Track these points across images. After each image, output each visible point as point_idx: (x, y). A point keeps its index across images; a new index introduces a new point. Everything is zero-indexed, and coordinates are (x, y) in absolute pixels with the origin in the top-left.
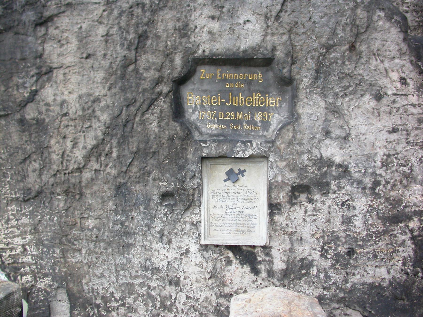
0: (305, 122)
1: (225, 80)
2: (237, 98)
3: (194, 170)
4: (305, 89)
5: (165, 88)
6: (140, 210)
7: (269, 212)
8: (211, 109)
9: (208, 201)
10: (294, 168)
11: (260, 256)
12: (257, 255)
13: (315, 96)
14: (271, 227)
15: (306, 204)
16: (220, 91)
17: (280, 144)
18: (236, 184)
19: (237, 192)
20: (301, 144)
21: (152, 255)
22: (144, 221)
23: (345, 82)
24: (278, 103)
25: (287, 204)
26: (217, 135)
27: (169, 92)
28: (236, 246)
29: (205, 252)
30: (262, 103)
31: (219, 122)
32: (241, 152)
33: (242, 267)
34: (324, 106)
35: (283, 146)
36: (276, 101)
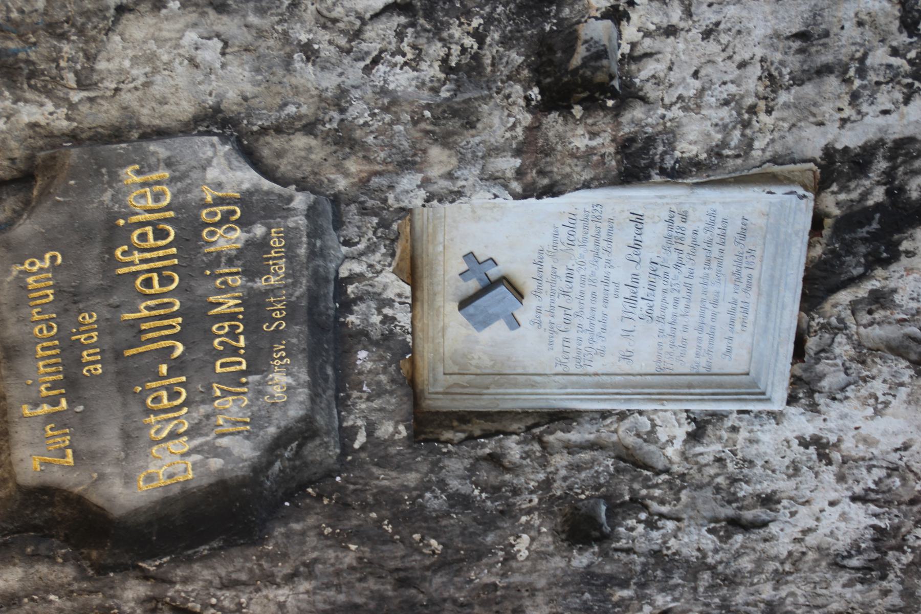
0: (234, 84)
1: (71, 383)
2: (144, 327)
3: (467, 463)
4: (72, 106)
6: (631, 599)
7: (657, 178)
8: (203, 402)
9: (601, 384)
10: (455, 113)
11: (864, 196)
12: (856, 208)
13: (102, 65)
14: (731, 163)
15: (630, 32)
16: (124, 389)
17: (346, 174)
18: (528, 286)
19: (562, 284)
20: (340, 99)
21: (819, 549)
22: (677, 585)
24: (155, 176)
25: (626, 117)
26: (316, 373)
27: (146, 576)
28: (808, 280)
29: (825, 384)
30: (160, 234)
31: (259, 362)
32: (387, 311)
33: (910, 254)
34: (150, 20)
35: (353, 166)
36: (144, 184)
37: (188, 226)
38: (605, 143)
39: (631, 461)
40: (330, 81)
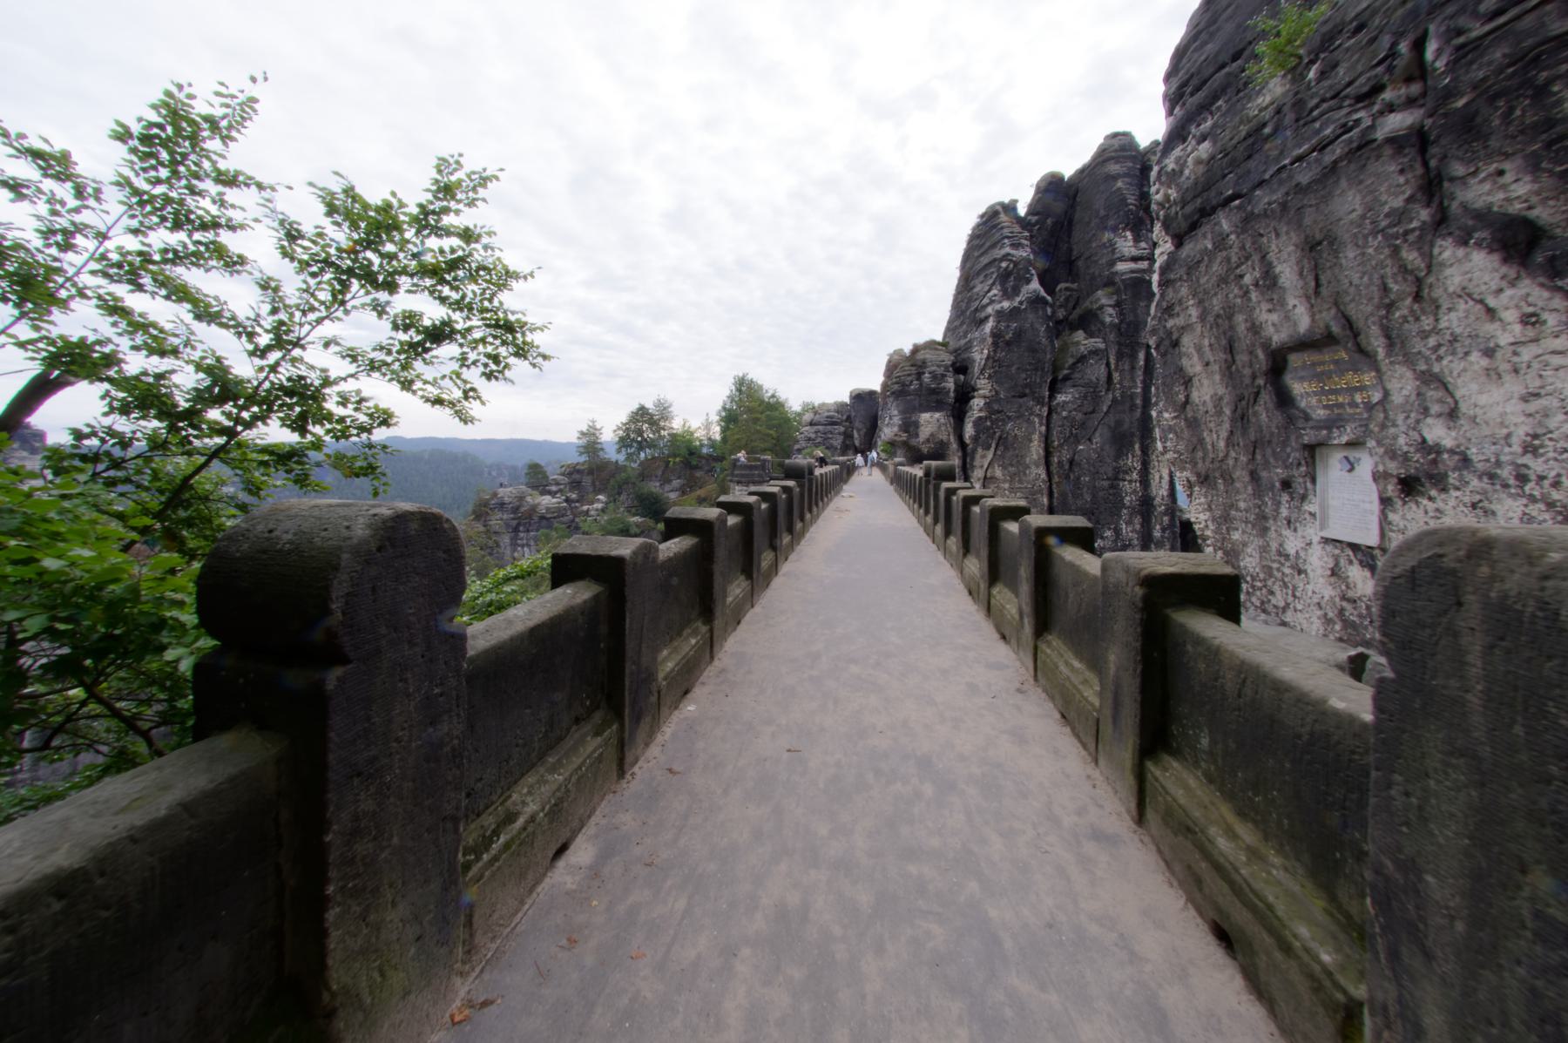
0: (1397, 399)
1: (1314, 364)
5: (1260, 381)
23: (1432, 342)
37: (1362, 389)
38: (1390, 494)
39: (1304, 498)
40: (1400, 422)
